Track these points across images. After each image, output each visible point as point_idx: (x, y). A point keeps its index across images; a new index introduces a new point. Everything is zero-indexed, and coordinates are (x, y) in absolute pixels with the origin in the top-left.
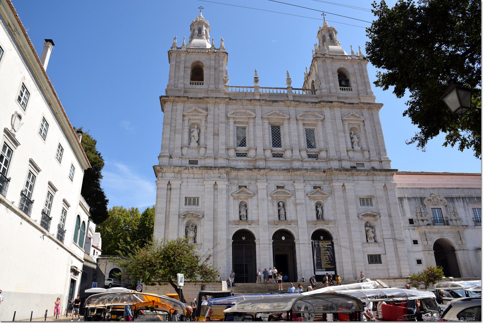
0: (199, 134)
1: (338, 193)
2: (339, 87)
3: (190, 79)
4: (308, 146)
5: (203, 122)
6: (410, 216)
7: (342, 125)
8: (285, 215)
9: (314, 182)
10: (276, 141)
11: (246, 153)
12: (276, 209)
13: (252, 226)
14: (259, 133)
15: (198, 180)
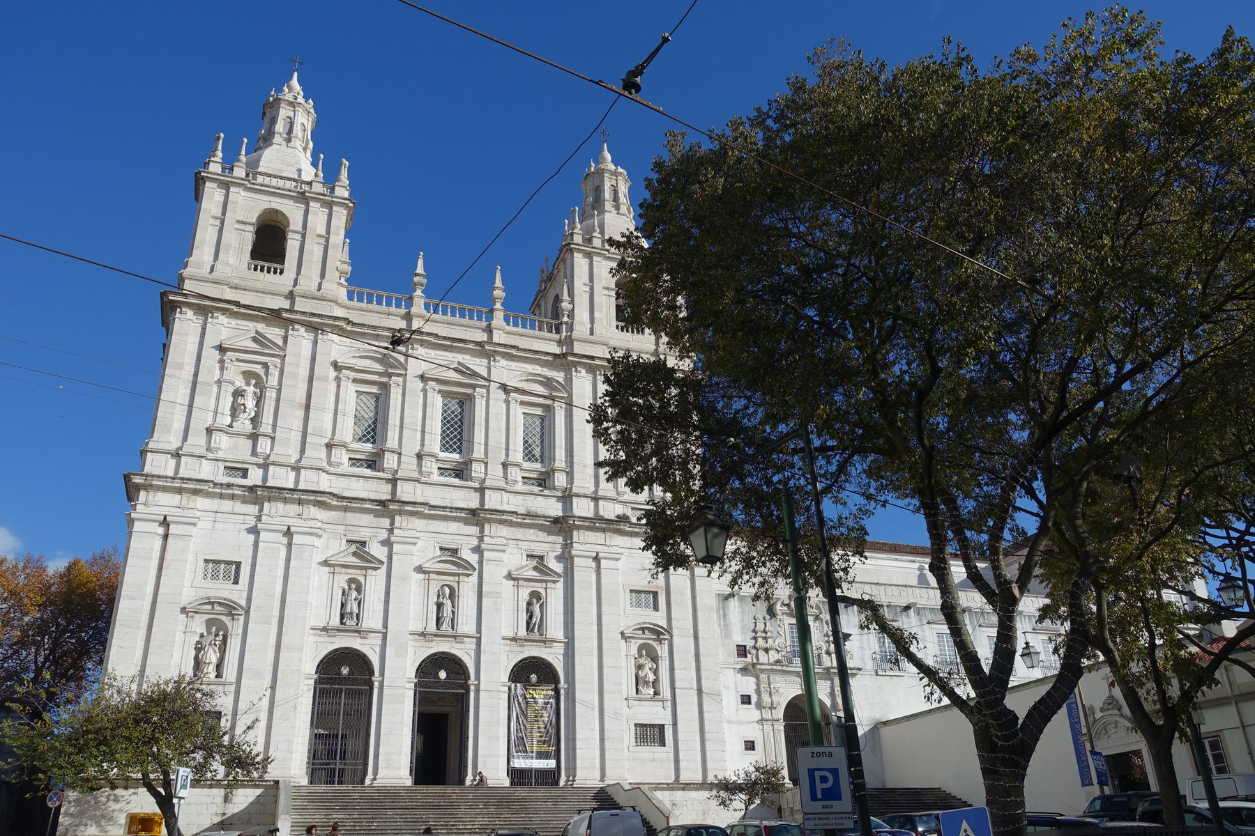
0: (259, 401)
2: (614, 323)
3: (248, 255)
4: (526, 455)
5: (275, 373)
6: (740, 639)
8: (453, 620)
9: (530, 543)
11: (374, 459)
13: (368, 641)
14: (414, 416)
15: (242, 517)
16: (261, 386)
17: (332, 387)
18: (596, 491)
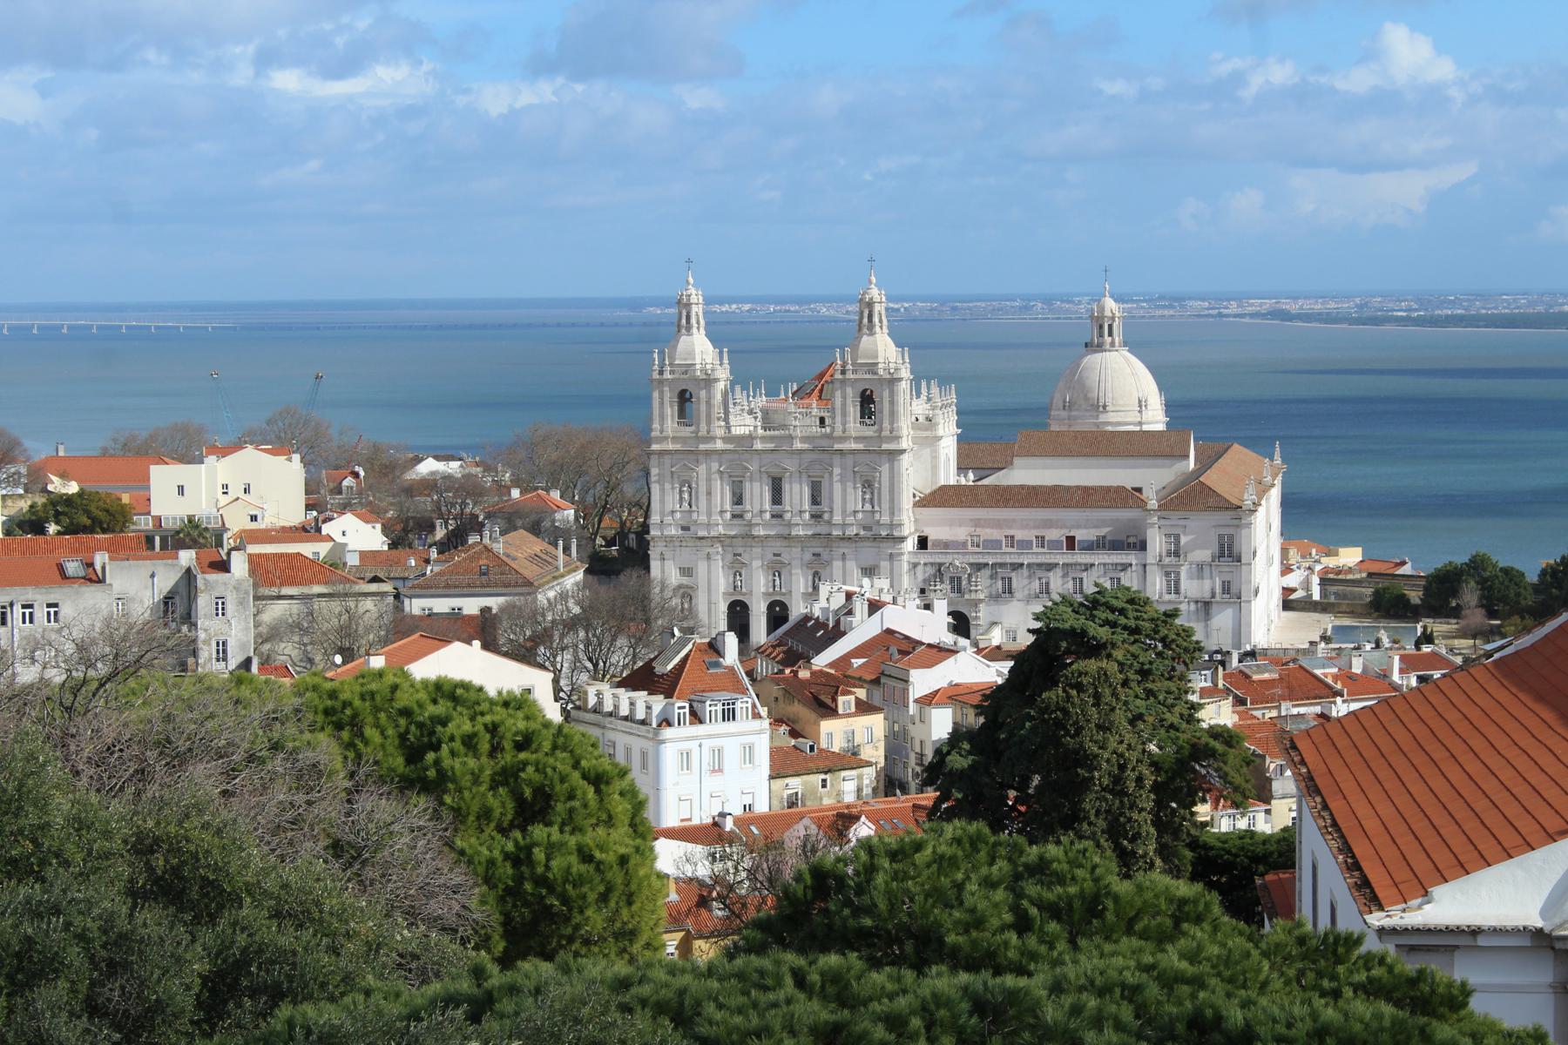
0: (690, 495)
1: (837, 564)
10: (777, 498)
12: (771, 578)
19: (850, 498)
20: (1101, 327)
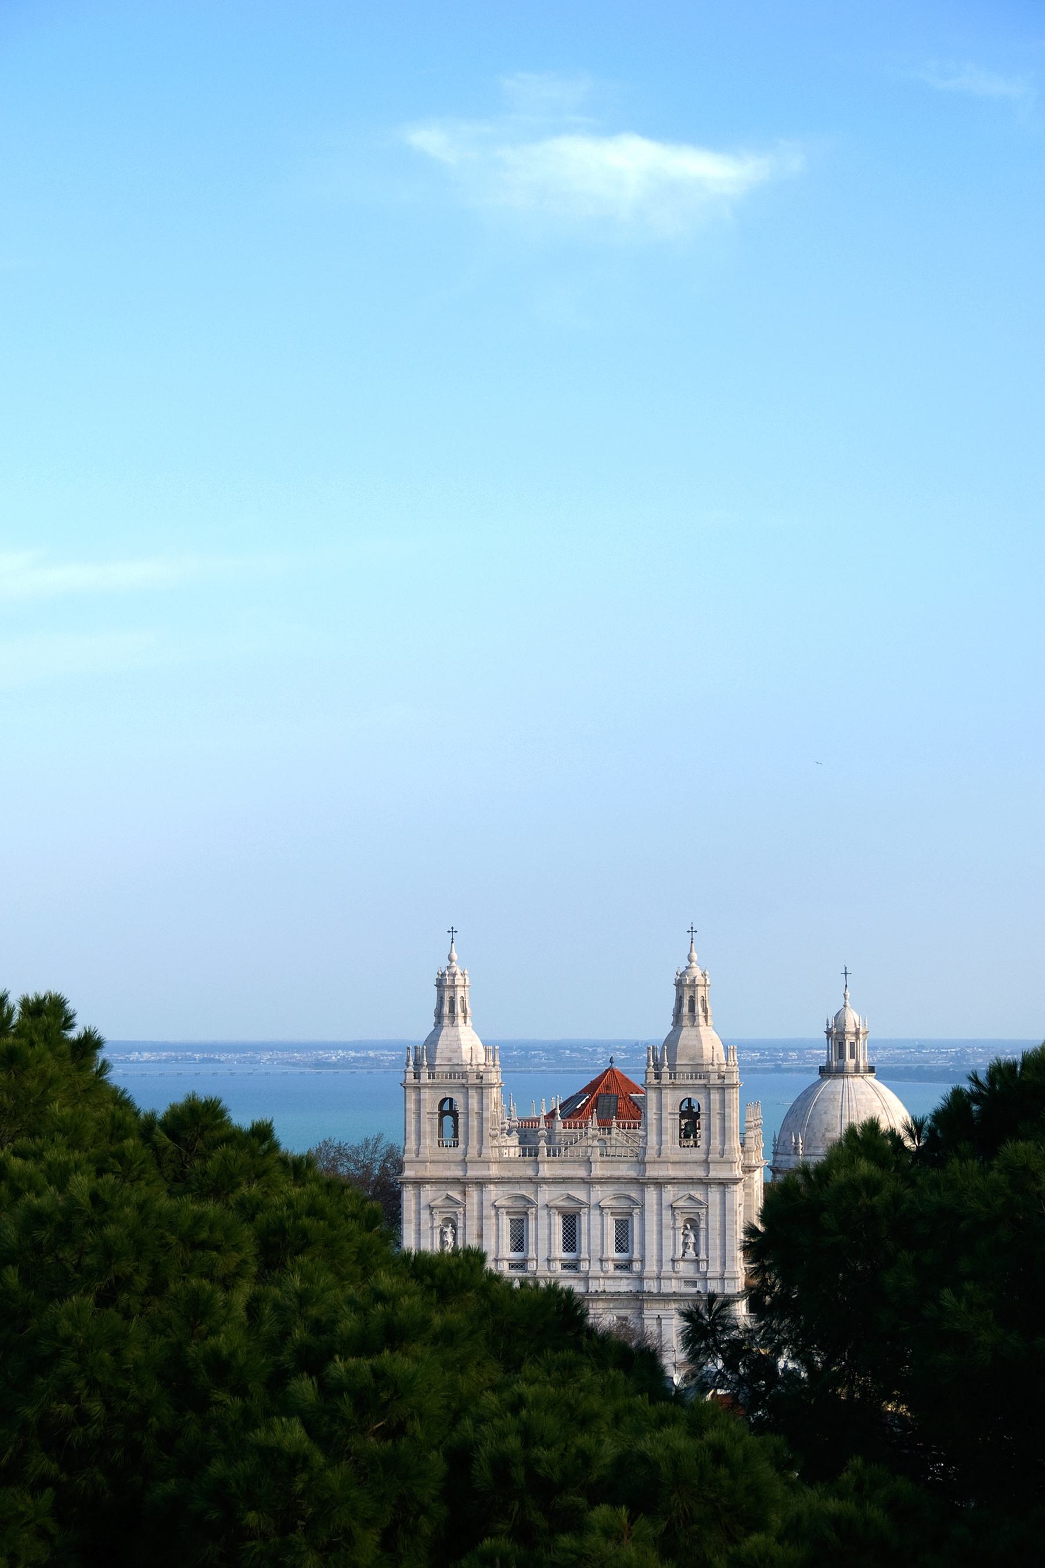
5: (461, 1217)
7: (670, 1217)
14: (543, 1233)
16: (454, 1227)
17: (494, 1221)
18: (660, 1272)
19: (667, 1243)
20: (841, 1046)
